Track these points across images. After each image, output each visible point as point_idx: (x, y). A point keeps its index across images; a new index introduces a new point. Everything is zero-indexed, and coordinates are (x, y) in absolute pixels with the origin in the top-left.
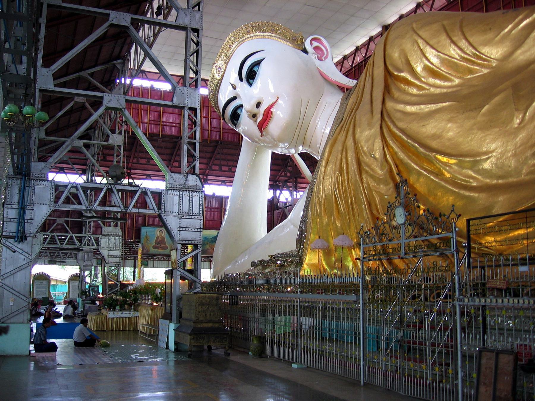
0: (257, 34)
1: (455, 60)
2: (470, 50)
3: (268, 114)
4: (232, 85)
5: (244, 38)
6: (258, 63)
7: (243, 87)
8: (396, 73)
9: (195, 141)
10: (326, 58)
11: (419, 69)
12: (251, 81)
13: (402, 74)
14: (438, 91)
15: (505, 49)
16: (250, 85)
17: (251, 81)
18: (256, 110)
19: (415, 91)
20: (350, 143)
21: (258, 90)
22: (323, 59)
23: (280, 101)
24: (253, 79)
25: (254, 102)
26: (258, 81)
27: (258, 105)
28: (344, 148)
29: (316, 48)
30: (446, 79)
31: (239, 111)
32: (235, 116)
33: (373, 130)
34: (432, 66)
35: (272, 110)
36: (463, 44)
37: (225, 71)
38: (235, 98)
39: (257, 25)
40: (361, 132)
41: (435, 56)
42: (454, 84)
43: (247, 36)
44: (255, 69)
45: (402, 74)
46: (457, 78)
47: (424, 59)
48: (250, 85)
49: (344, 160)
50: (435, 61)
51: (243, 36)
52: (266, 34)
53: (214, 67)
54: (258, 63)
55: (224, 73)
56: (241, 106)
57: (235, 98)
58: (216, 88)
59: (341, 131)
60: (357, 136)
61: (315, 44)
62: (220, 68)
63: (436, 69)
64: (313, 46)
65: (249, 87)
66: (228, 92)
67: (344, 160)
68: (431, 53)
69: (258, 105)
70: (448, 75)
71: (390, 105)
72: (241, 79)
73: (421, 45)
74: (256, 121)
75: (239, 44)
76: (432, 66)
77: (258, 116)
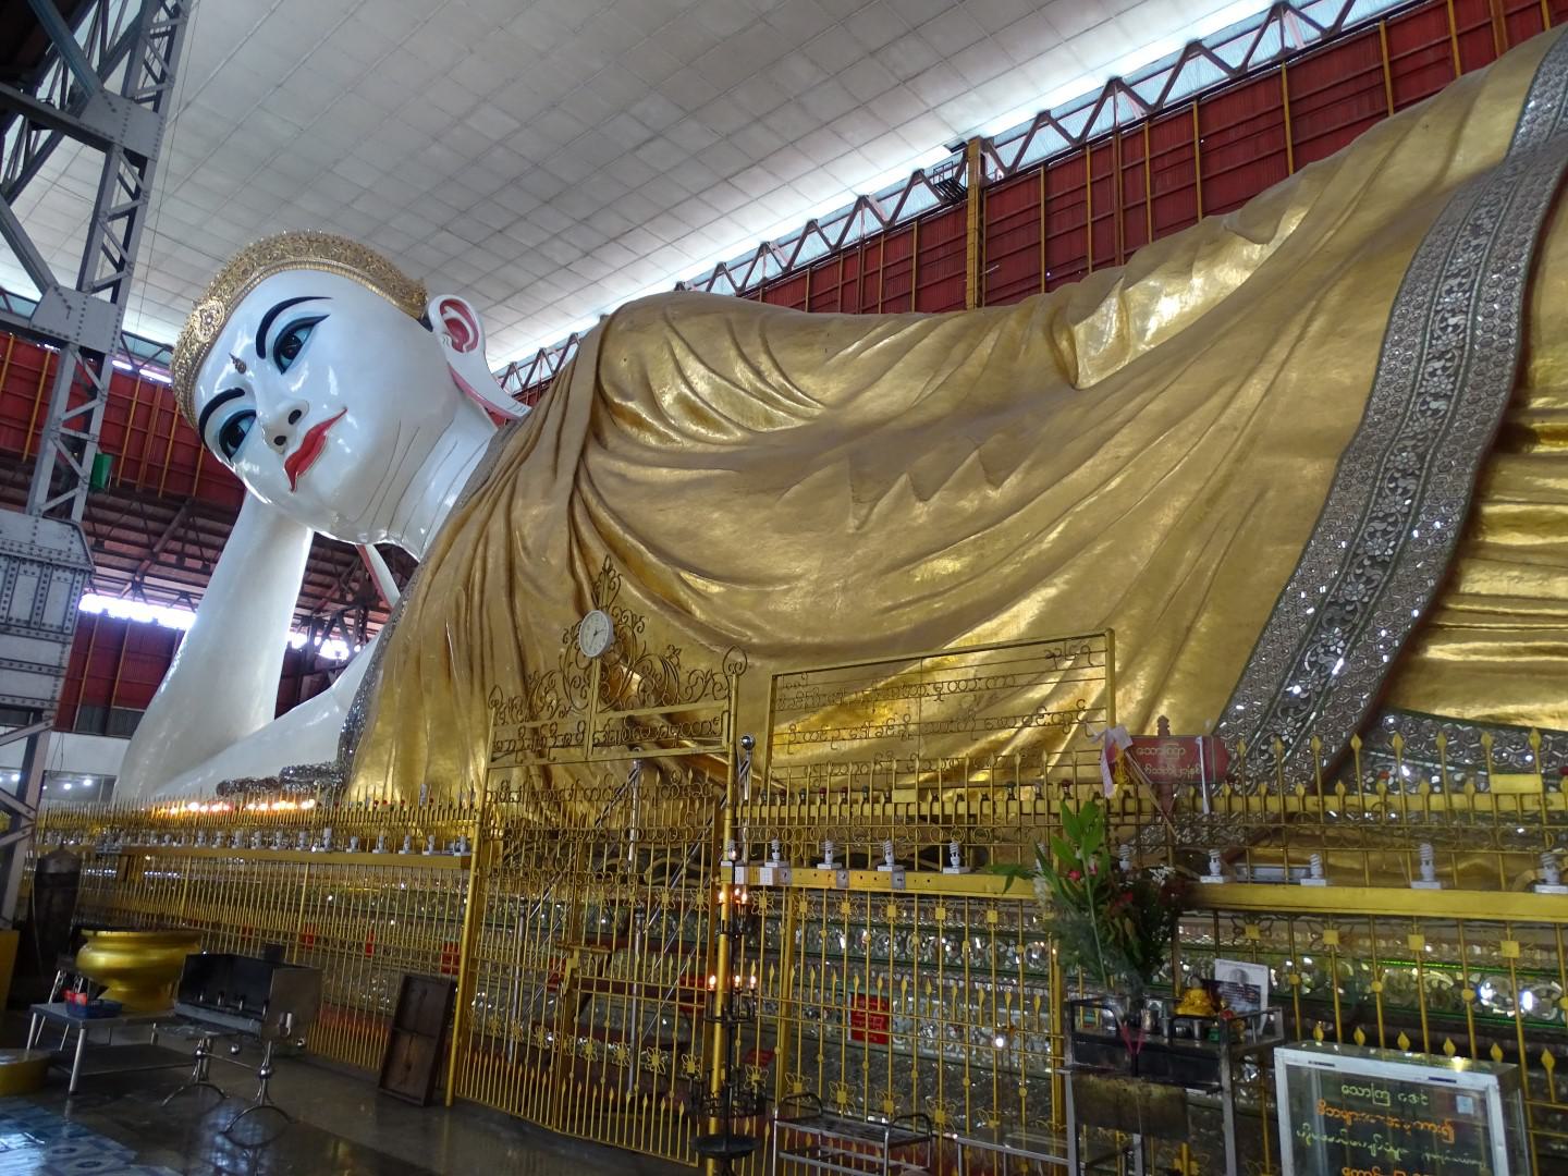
0: (313, 259)
1: (742, 393)
2: (775, 378)
3: (314, 443)
4: (236, 361)
6: (309, 324)
7: (261, 373)
8: (617, 400)
9: (83, 436)
10: (472, 347)
11: (667, 400)
12: (285, 360)
13: (631, 405)
14: (700, 447)
15: (842, 386)
16: (283, 369)
18: (286, 428)
19: (652, 441)
20: (497, 526)
21: (299, 384)
22: (464, 347)
23: (349, 418)
24: (292, 356)
25: (284, 408)
26: (303, 366)
27: (295, 416)
28: (483, 535)
30: (718, 428)
31: (244, 425)
32: (233, 436)
33: (550, 507)
34: (693, 398)
35: (326, 433)
36: (765, 364)
37: (222, 327)
38: (238, 393)
40: (526, 507)
41: (703, 377)
42: (732, 438)
44: (301, 335)
45: (631, 405)
46: (739, 426)
47: (679, 381)
48: (283, 369)
49: (478, 563)
50: (702, 387)
51: (283, 257)
52: (340, 264)
53: (197, 313)
54: (309, 324)
55: (220, 332)
56: (251, 415)
57: (238, 393)
58: (194, 360)
59: (480, 501)
60: (516, 514)
61: (452, 313)
62: (211, 316)
63: (701, 404)
64: (447, 316)
65: (279, 373)
66: (223, 375)
67: (478, 563)
68: (696, 372)
69: (295, 416)
70: (723, 420)
71: (596, 459)
72: (261, 352)
73: (677, 351)
74: (283, 452)
75: (269, 272)
76: (693, 398)
77: (289, 441)
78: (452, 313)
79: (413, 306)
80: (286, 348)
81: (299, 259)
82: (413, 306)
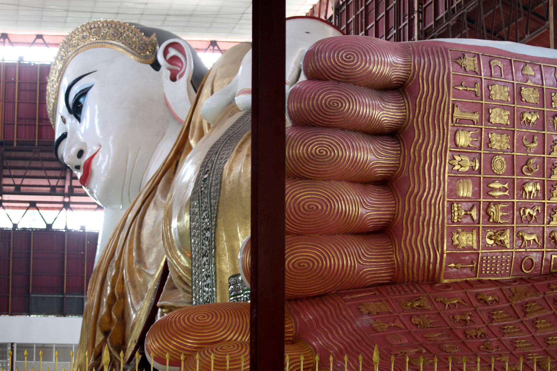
5: (78, 47)
6: (84, 93)
10: (181, 76)
16: (79, 119)
17: (79, 115)
22: (177, 77)
25: (74, 150)
27: (80, 154)
29: (173, 60)
35: (94, 161)
39: (96, 26)
43: (83, 44)
44: (81, 100)
48: (79, 119)
52: (106, 41)
54: (84, 93)
61: (173, 52)
64: (169, 56)
69: (80, 154)
72: (70, 111)
78: (173, 52)
79: (146, 57)
80: (76, 110)
81: (86, 43)
82: (146, 57)
